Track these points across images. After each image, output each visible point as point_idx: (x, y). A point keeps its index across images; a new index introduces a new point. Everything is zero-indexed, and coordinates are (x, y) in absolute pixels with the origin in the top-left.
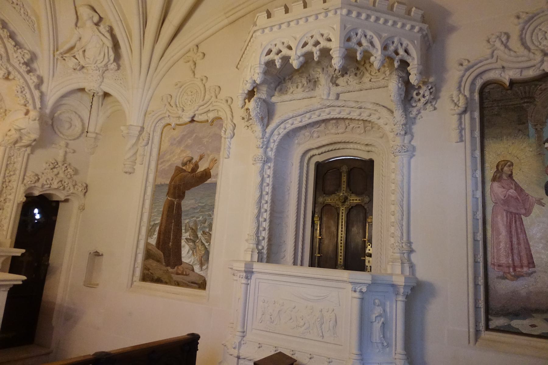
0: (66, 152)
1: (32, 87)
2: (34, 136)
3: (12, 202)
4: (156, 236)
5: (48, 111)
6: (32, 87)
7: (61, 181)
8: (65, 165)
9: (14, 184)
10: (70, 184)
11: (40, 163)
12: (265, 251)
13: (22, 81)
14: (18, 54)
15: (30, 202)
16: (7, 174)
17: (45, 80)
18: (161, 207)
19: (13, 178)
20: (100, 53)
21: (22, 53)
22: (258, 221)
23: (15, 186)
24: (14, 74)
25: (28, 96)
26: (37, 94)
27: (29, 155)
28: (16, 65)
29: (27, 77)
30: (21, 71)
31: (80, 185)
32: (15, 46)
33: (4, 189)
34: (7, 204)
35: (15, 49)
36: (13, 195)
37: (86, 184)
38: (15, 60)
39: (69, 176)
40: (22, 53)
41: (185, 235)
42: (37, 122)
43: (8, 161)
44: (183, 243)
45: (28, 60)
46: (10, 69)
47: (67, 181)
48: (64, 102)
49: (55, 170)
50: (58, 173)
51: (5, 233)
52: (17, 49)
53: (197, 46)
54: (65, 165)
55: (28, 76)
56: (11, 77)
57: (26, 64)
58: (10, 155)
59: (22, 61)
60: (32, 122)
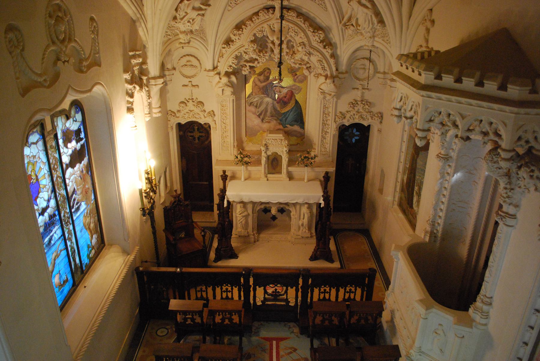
0: (363, 93)
1: (328, 57)
2: (333, 94)
3: (329, 134)
4: (406, 177)
5: (343, 68)
6: (328, 57)
7: (361, 115)
8: (363, 102)
9: (329, 122)
10: (368, 116)
11: (343, 106)
12: (439, 235)
15: (344, 132)
17: (338, 46)
18: (409, 156)
19: (330, 118)
20: (365, 21)
22: (435, 210)
25: (326, 65)
26: (332, 61)
27: (336, 103)
28: (316, 46)
30: (320, 48)
31: (376, 115)
32: (314, 32)
36: (330, 129)
37: (380, 113)
39: (367, 110)
41: (416, 188)
44: (415, 194)
46: (311, 51)
47: (365, 114)
48: (356, 55)
49: (355, 108)
50: (359, 109)
53: (431, 10)
54: (363, 102)
59: (319, 41)
60: (329, 85)
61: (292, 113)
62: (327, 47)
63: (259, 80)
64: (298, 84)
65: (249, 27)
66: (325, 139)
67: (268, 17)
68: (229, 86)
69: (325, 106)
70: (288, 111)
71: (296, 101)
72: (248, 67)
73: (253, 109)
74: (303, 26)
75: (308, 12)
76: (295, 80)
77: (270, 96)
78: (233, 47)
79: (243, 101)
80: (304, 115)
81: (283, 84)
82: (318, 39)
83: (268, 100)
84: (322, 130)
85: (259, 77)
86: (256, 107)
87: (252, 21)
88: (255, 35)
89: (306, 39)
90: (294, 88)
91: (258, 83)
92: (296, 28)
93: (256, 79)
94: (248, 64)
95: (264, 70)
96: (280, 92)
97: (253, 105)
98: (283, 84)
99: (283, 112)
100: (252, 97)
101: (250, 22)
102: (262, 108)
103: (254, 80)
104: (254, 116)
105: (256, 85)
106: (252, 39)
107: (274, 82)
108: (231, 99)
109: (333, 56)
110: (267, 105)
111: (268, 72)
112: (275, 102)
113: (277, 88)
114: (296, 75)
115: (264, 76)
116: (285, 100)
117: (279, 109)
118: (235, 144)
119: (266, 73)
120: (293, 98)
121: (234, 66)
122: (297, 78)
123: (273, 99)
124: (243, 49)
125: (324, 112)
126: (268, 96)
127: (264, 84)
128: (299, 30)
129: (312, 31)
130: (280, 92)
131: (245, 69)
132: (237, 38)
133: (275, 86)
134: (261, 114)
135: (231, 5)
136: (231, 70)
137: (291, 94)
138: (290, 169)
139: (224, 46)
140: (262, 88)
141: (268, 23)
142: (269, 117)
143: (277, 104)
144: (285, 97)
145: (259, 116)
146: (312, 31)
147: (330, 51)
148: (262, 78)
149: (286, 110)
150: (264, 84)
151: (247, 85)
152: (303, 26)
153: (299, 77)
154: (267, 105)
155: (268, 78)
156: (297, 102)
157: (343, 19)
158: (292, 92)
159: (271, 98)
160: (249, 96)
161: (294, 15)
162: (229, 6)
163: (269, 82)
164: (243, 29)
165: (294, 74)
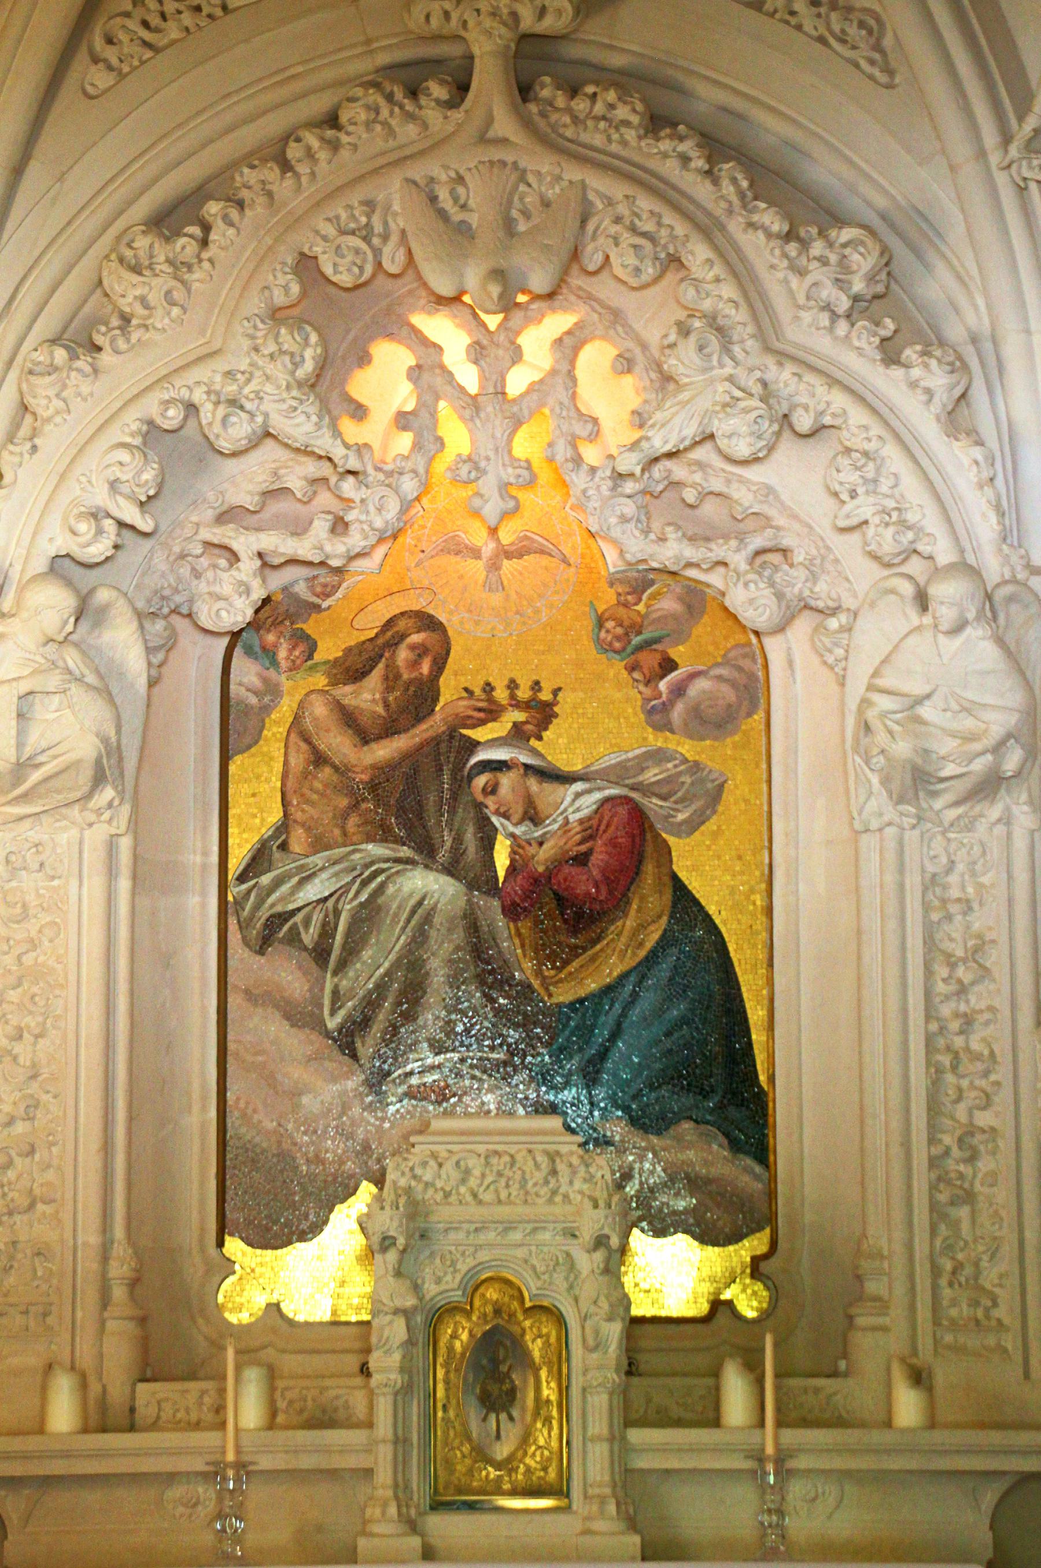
13: (857, 416)
14: (817, 273)
16: (941, 987)
21: (833, 258)
23: (1002, 1048)
24: (810, 398)
29: (887, 383)
32: (789, 236)
33: (950, 1078)
34: (985, 1164)
35: (792, 248)
38: (807, 316)
40: (833, 258)
42: (977, 634)
43: (927, 907)
45: (871, 279)
51: (1010, 1342)
52: (804, 244)
55: (897, 372)
56: (804, 422)
57: (862, 308)
58: (931, 869)
59: (844, 304)
60: (951, 645)
61: (648, 1001)
62: (910, 354)
63: (348, 718)
64: (687, 748)
65: (257, 211)
66: (969, 1197)
67: (412, 130)
68: (79, 680)
69: (931, 882)
70: (608, 990)
71: (679, 888)
72: (248, 566)
73: (287, 973)
74: (702, 191)
75: (738, 104)
76: (657, 715)
77: (443, 855)
78: (123, 368)
79: (202, 907)
80: (756, 1014)
81: (558, 746)
82: (828, 292)
83: (425, 884)
84: (934, 1108)
85: (346, 693)
86: (321, 954)
87: (286, 167)
88: (306, 265)
89: (728, 290)
90: (652, 775)
91: (339, 743)
92: (645, 203)
93: (320, 709)
94: (246, 543)
95: (390, 636)
96: (532, 816)
97: (294, 939)
98: (558, 746)
99: (564, 995)
100: (283, 865)
101: (271, 173)
102: (375, 961)
103: (297, 719)
104: (296, 1042)
105: (319, 759)
106: (279, 298)
107: (479, 734)
108: (98, 834)
109: (957, 418)
110: (420, 937)
111: (421, 651)
112: (492, 908)
113: (507, 781)
114: (668, 665)
115: (391, 679)
116: (584, 884)
117: (525, 969)
118: (119, 1270)
119: (403, 654)
120: (649, 868)
121: (131, 514)
122: (679, 690)
123: (471, 886)
124: (210, 373)
125: (930, 942)
126: (426, 851)
127: (384, 751)
128: (669, 218)
129: (778, 226)
130: (532, 816)
131: (226, 582)
132: (155, 287)
133: (487, 766)
134: (359, 1024)
135: (111, 54)
136: (99, 550)
137: (631, 838)
138: (655, 1446)
139: (40, 357)
140: (373, 787)
141: (417, 171)
142: (438, 1048)
143: (501, 922)
144: (582, 860)
145: (346, 1041)
146: (778, 226)
147: (938, 379)
148: (367, 696)
149: (592, 986)
150: (384, 751)
151: (232, 768)
152: (702, 191)
153: (699, 687)
154: (420, 937)
155: (421, 698)
156: (684, 902)
157: (1021, 119)
158: (638, 821)
159: (451, 870)
160: (259, 860)
161: (622, 112)
162: (96, 60)
163: (434, 725)
164: (207, 228)
165: (650, 660)
